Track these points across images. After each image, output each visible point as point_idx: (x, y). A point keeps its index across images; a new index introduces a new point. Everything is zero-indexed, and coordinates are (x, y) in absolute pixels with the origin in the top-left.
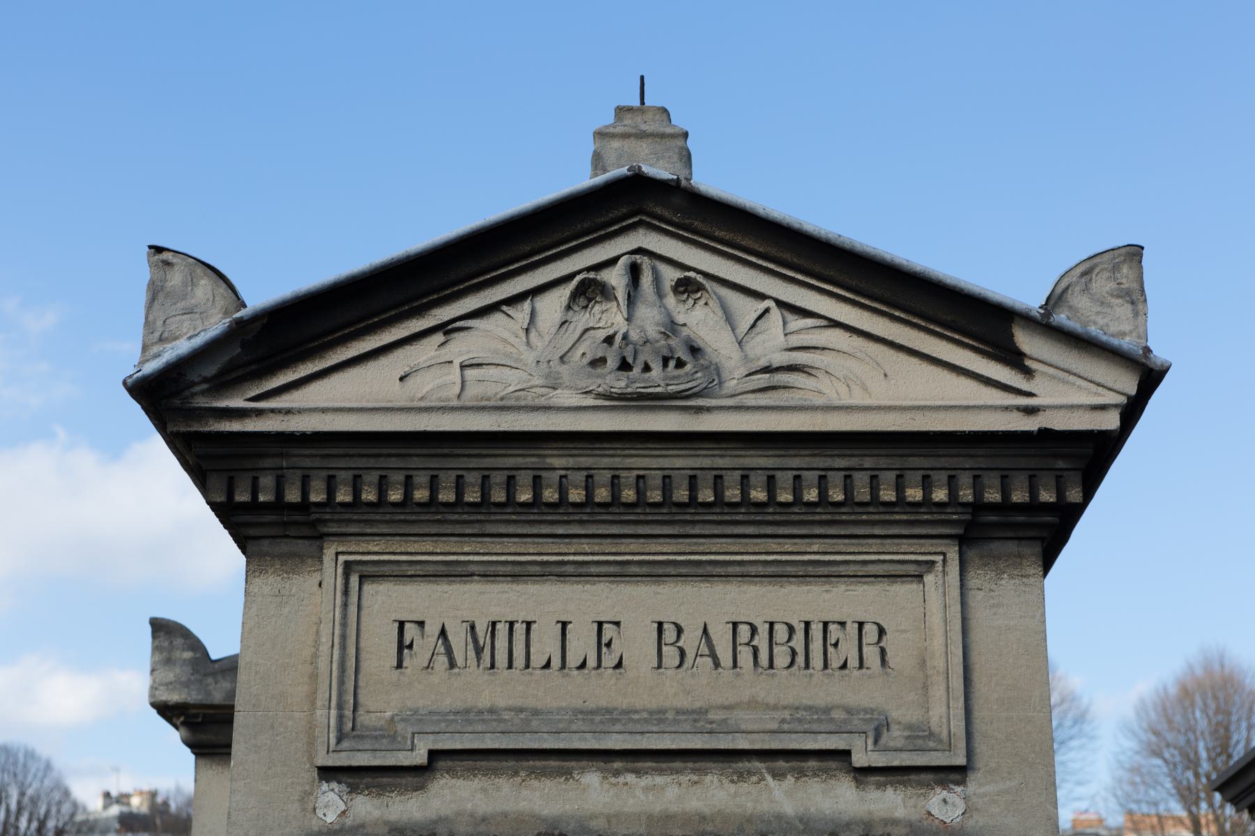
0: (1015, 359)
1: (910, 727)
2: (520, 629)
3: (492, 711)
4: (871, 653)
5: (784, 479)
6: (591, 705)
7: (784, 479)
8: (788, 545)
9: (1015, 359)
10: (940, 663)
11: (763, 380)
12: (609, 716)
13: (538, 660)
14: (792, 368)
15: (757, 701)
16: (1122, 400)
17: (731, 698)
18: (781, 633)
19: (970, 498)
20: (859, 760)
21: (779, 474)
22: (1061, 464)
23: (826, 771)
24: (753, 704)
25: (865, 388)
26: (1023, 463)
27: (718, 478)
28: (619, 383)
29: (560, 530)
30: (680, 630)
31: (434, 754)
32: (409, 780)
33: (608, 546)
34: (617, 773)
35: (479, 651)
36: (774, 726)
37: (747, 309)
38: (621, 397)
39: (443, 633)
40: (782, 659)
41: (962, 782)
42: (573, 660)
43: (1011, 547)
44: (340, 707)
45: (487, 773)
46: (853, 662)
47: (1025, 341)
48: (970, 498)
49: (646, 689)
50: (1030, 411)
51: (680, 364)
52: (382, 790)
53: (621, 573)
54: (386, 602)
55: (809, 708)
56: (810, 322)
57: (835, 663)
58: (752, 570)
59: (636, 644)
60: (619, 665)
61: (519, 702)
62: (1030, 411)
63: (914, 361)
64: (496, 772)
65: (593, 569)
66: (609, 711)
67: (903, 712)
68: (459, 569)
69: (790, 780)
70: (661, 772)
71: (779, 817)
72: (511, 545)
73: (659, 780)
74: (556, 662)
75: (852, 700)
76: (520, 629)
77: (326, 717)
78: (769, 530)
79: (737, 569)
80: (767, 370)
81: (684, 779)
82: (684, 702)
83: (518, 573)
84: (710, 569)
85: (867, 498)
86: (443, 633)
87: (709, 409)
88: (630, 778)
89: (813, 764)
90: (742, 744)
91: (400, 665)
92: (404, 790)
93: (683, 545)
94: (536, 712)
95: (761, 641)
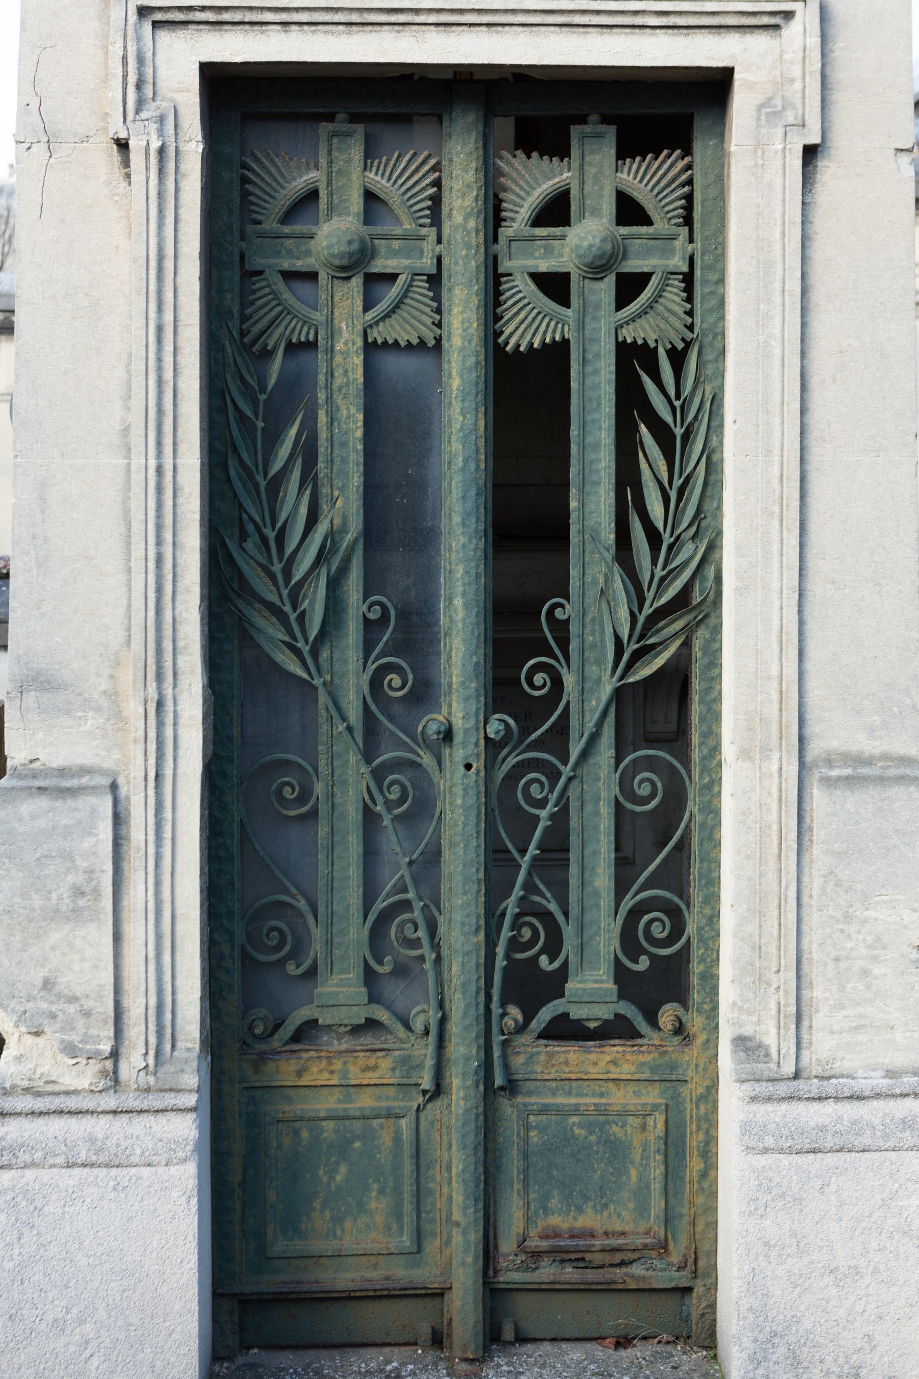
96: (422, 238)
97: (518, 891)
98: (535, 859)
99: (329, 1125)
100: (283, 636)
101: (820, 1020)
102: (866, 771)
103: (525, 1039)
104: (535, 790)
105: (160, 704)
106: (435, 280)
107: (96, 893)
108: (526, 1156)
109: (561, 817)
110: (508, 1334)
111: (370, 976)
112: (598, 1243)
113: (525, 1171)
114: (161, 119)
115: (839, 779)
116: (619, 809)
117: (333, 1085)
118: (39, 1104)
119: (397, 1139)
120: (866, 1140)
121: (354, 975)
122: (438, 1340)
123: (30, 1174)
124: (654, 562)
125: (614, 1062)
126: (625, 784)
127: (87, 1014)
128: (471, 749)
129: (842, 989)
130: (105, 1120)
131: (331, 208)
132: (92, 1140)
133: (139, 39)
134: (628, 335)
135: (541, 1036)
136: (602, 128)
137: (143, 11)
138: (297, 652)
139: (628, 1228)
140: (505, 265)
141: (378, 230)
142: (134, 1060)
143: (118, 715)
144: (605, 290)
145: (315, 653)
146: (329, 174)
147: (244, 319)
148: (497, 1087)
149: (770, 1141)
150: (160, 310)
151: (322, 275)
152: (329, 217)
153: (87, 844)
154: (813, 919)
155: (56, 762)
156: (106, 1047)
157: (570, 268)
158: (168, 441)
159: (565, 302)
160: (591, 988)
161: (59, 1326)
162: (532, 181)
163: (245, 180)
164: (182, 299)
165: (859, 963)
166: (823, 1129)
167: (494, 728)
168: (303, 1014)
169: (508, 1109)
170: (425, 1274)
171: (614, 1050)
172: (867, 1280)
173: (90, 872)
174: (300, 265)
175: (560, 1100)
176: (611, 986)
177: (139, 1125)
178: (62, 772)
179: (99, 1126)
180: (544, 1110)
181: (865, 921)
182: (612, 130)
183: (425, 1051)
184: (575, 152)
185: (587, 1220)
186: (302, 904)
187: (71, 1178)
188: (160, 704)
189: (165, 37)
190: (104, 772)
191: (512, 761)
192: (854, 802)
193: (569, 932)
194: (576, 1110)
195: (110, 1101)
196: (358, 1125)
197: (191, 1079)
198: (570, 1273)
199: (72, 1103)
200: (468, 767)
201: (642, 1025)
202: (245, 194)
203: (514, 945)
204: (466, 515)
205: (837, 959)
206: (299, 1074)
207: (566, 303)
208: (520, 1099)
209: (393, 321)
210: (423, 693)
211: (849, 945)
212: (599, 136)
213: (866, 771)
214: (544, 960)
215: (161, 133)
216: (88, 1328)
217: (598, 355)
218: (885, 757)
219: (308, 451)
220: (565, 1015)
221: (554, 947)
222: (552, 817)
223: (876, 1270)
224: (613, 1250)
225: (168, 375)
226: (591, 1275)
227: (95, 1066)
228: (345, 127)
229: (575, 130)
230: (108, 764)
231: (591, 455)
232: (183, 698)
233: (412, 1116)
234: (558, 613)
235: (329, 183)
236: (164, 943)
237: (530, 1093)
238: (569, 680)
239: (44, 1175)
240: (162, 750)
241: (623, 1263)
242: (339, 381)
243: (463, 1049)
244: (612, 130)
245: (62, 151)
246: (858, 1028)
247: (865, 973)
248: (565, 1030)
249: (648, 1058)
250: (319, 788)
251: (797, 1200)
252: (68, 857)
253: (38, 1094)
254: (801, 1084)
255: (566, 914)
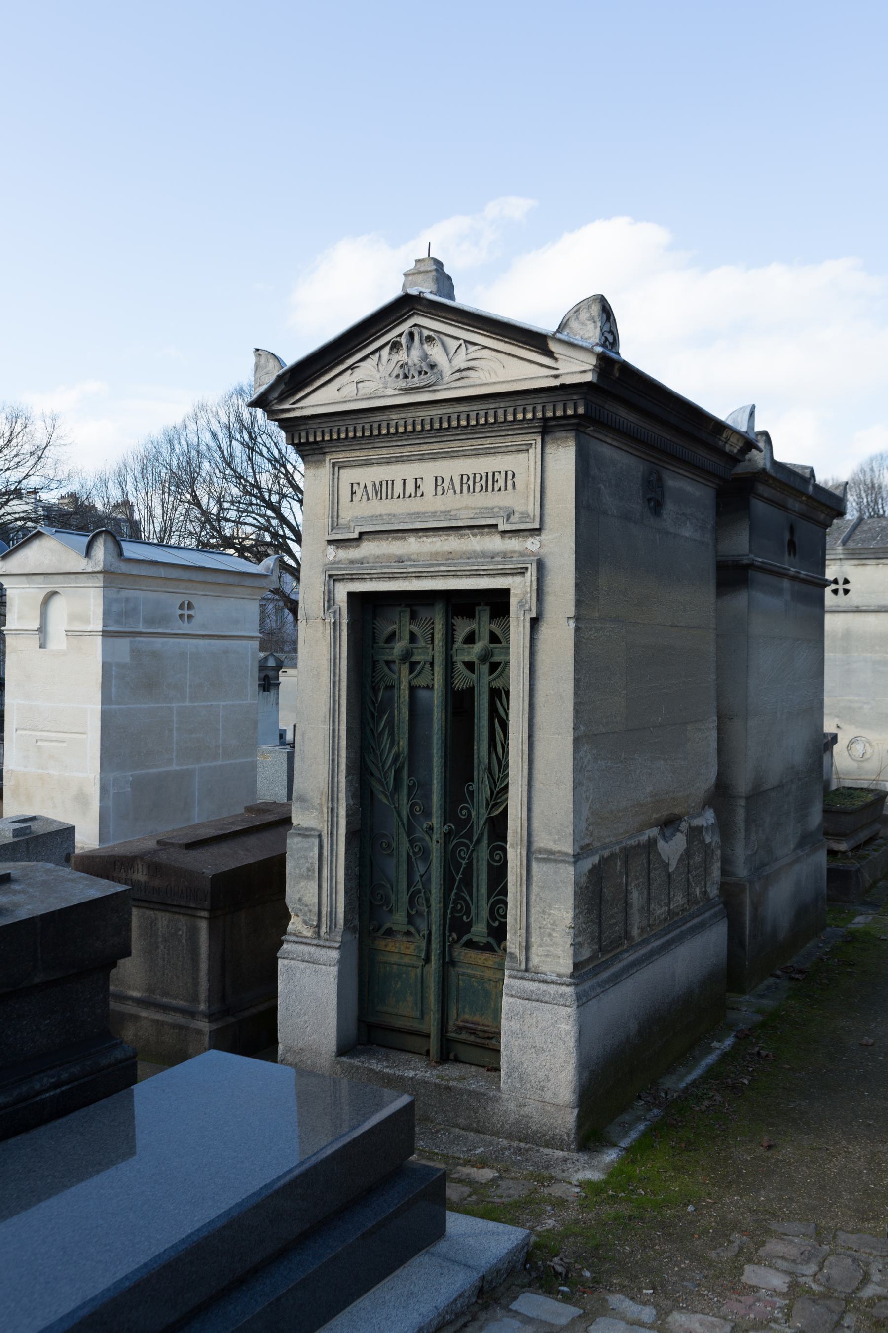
0: (550, 354)
1: (522, 513)
2: (390, 483)
3: (380, 516)
4: (510, 483)
5: (473, 415)
6: (412, 512)
7: (473, 415)
8: (479, 442)
9: (550, 354)
10: (532, 486)
11: (458, 375)
12: (418, 515)
13: (396, 495)
14: (469, 369)
15: (466, 506)
16: (592, 367)
17: (459, 505)
18: (478, 477)
19: (541, 416)
20: (501, 528)
21: (480, 412)
22: (575, 397)
23: (491, 533)
24: (467, 508)
25: (496, 373)
26: (560, 398)
27: (449, 417)
28: (403, 384)
29: (399, 444)
30: (443, 481)
31: (361, 534)
32: (354, 543)
33: (417, 448)
34: (420, 537)
35: (377, 493)
36: (472, 516)
37: (452, 344)
38: (406, 389)
39: (365, 486)
40: (478, 489)
41: (539, 535)
42: (407, 495)
43: (564, 434)
44: (332, 517)
45: (378, 539)
46: (503, 488)
47: (553, 346)
48: (541, 416)
49: (432, 505)
50: (556, 377)
51: (426, 373)
52: (346, 547)
53: (422, 458)
54: (348, 476)
55: (486, 508)
56: (477, 347)
57: (496, 489)
58: (467, 453)
59: (428, 486)
60: (422, 495)
61: (388, 512)
62: (556, 377)
63: (515, 359)
64: (381, 539)
65: (413, 458)
66: (418, 513)
67: (519, 508)
68: (369, 462)
69: (478, 537)
70: (435, 536)
71: (474, 552)
72: (385, 451)
73: (434, 539)
74: (401, 496)
75: (501, 504)
76: (390, 483)
77: (327, 522)
78: (471, 436)
79: (462, 453)
80: (459, 371)
81: (442, 538)
82: (443, 509)
83: (388, 462)
84: (452, 454)
85: (502, 420)
86: (365, 486)
87: (438, 390)
88: (425, 539)
89: (486, 530)
90: (460, 524)
91: (352, 500)
92: (353, 547)
93: (442, 445)
94: (394, 515)
95: (471, 483)
96: (428, 649)
97: (455, 891)
98: (460, 879)
99: (395, 967)
100: (381, 789)
101: (534, 950)
102: (552, 857)
103: (457, 946)
104: (462, 853)
105: (332, 809)
106: (432, 664)
107: (314, 870)
108: (458, 990)
109: (470, 865)
110: (452, 1056)
111: (409, 915)
112: (479, 1028)
113: (458, 995)
114: (335, 612)
115: (541, 858)
116: (489, 864)
117: (400, 952)
118: (296, 939)
119: (416, 975)
120: (547, 999)
121: (404, 914)
122: (428, 1053)
123: (292, 962)
124: (499, 771)
125: (486, 960)
126: (491, 854)
127: (310, 911)
128: (438, 836)
129: (542, 940)
130: (314, 948)
131: (400, 638)
132: (310, 954)
133: (329, 585)
134: (494, 685)
135: (463, 946)
136: (485, 607)
137: (330, 576)
138: (386, 796)
139: (490, 1024)
140: (455, 658)
141: (414, 645)
142: (323, 929)
143: (322, 812)
144: (485, 668)
145: (392, 796)
146: (399, 626)
147: (373, 677)
148: (448, 963)
149: (513, 993)
150: (334, 676)
151: (397, 661)
152: (399, 641)
153: (311, 854)
154: (533, 911)
155: (305, 826)
156: (315, 923)
157: (475, 659)
158: (337, 720)
159: (473, 672)
160: (479, 930)
161: (299, 1015)
162: (463, 628)
163: (374, 628)
164: (342, 673)
165: (548, 930)
166: (532, 992)
167: (445, 829)
168: (388, 925)
169: (453, 972)
170: (423, 1028)
171: (486, 955)
172: (546, 1053)
173: (312, 863)
174: (390, 658)
175: (469, 971)
176: (486, 930)
177: (323, 951)
178: (307, 829)
179: (313, 949)
180: (463, 974)
181: (550, 914)
182: (488, 608)
183: (424, 945)
184: (477, 617)
185: (476, 1018)
186: (388, 885)
187: (303, 965)
188: (332, 809)
189: (338, 584)
190: (318, 831)
191: (455, 842)
192: (547, 868)
193: (473, 908)
194: (473, 976)
195: (315, 942)
196: (404, 968)
197: (339, 939)
198: (472, 1038)
199: (305, 940)
200: (438, 842)
201: (496, 948)
202: (374, 633)
203: (454, 910)
204: (438, 750)
205: (540, 928)
206: (386, 946)
207: (473, 673)
208: (457, 969)
209: (419, 678)
210: (428, 814)
211: (545, 923)
212: (485, 610)
213: (552, 857)
214: (465, 918)
215: (334, 617)
216: (307, 1017)
217: (484, 692)
218: (560, 852)
219: (390, 723)
220: (471, 939)
221: (468, 913)
222: (466, 863)
223: (549, 1050)
224: (485, 1032)
225: (337, 698)
226: (478, 1040)
227: (312, 930)
228: (403, 609)
229: (477, 608)
230: (319, 828)
231: (481, 730)
232: (340, 808)
233: (420, 968)
234: (470, 788)
235: (399, 629)
236: (333, 891)
237: (460, 967)
238: (474, 813)
239: (296, 963)
240: (333, 824)
241: (489, 1038)
242: (402, 699)
243: (435, 946)
244: (488, 608)
245: (310, 622)
246: (547, 956)
247: (550, 935)
248: (471, 945)
249: (497, 960)
250: (394, 845)
251: (522, 1017)
252: (306, 858)
253: (297, 936)
254: (527, 974)
255: (472, 900)
